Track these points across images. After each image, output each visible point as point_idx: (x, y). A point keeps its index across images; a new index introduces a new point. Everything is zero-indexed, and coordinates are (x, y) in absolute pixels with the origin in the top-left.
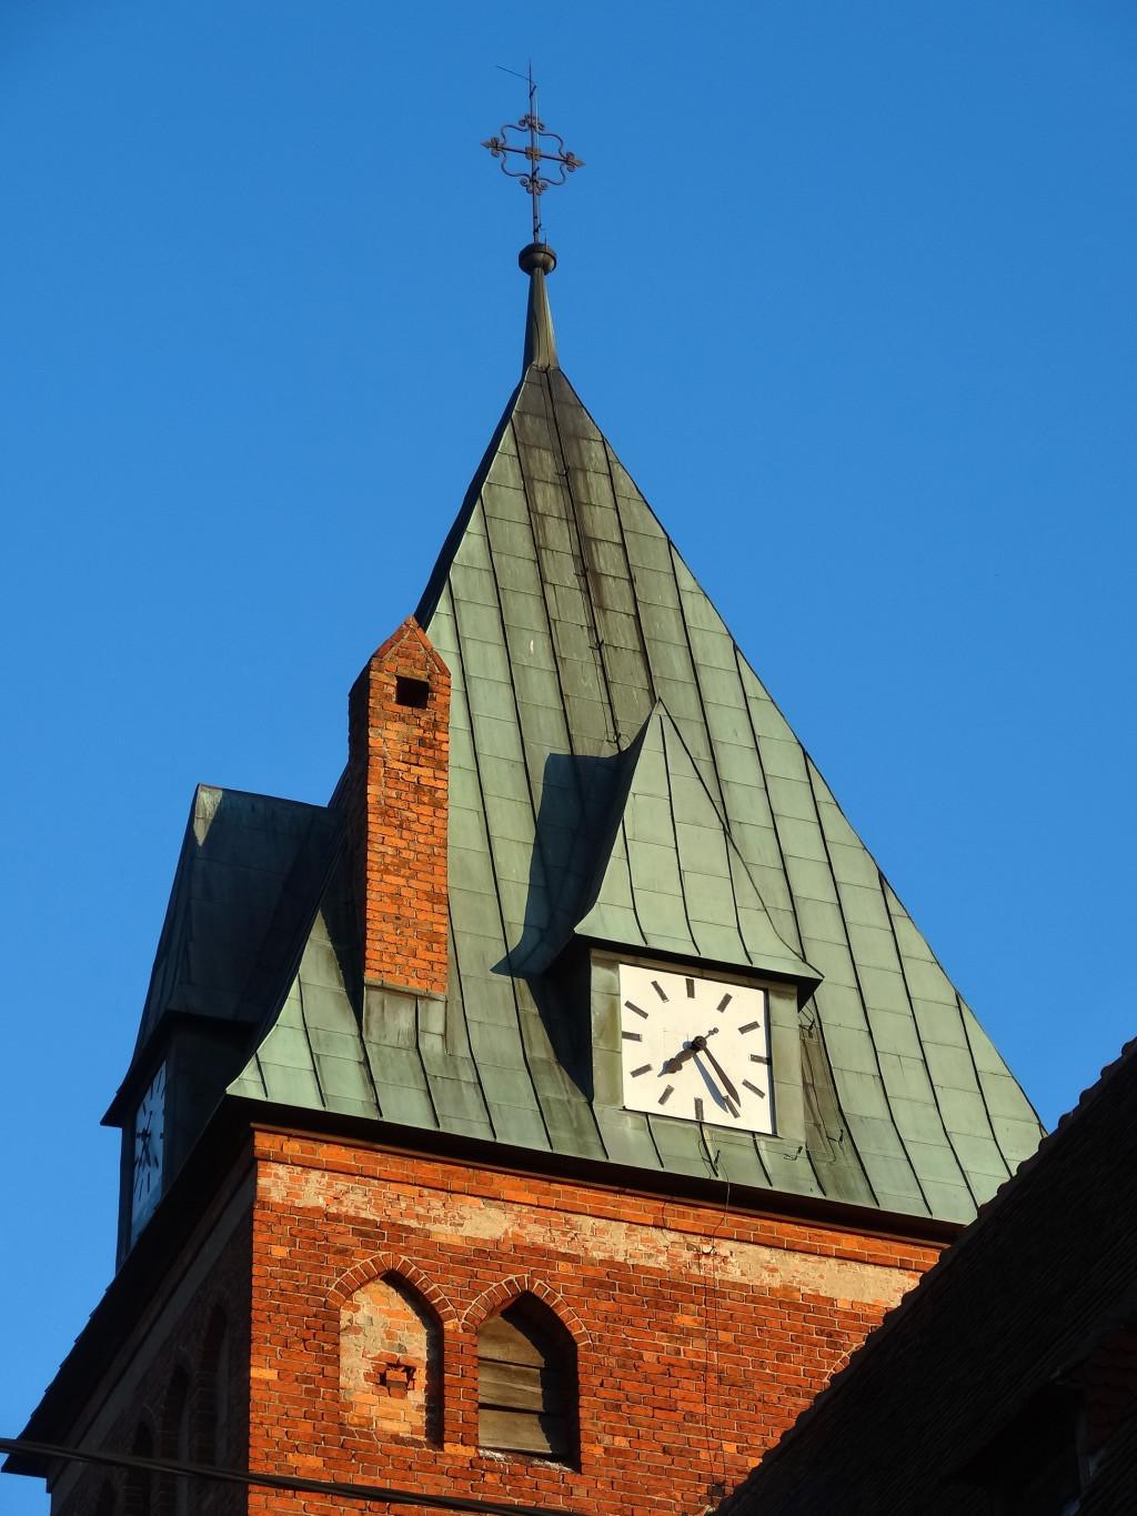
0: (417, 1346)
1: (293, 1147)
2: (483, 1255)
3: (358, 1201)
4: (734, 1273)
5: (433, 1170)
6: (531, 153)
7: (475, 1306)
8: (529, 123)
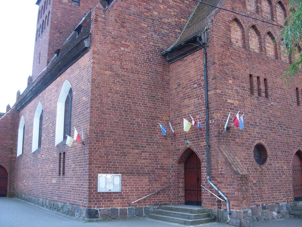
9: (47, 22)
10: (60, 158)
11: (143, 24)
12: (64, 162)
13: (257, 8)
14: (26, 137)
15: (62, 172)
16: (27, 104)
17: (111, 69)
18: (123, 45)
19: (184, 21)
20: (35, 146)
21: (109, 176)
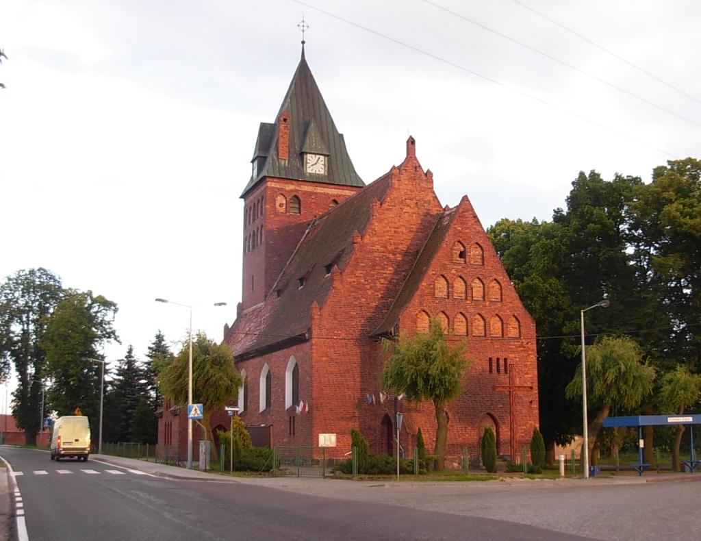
0: (284, 202)
1: (271, 180)
2: (292, 191)
3: (278, 186)
4: (318, 191)
5: (285, 181)
6: (303, 26)
7: (290, 197)
8: (303, 22)
9: (259, 235)
10: (290, 421)
11: (352, 313)
12: (294, 425)
13: (448, 293)
14: (250, 395)
15: (292, 432)
16: (248, 359)
17: (327, 356)
18: (335, 335)
19: (391, 301)
20: (262, 406)
21: (327, 435)
